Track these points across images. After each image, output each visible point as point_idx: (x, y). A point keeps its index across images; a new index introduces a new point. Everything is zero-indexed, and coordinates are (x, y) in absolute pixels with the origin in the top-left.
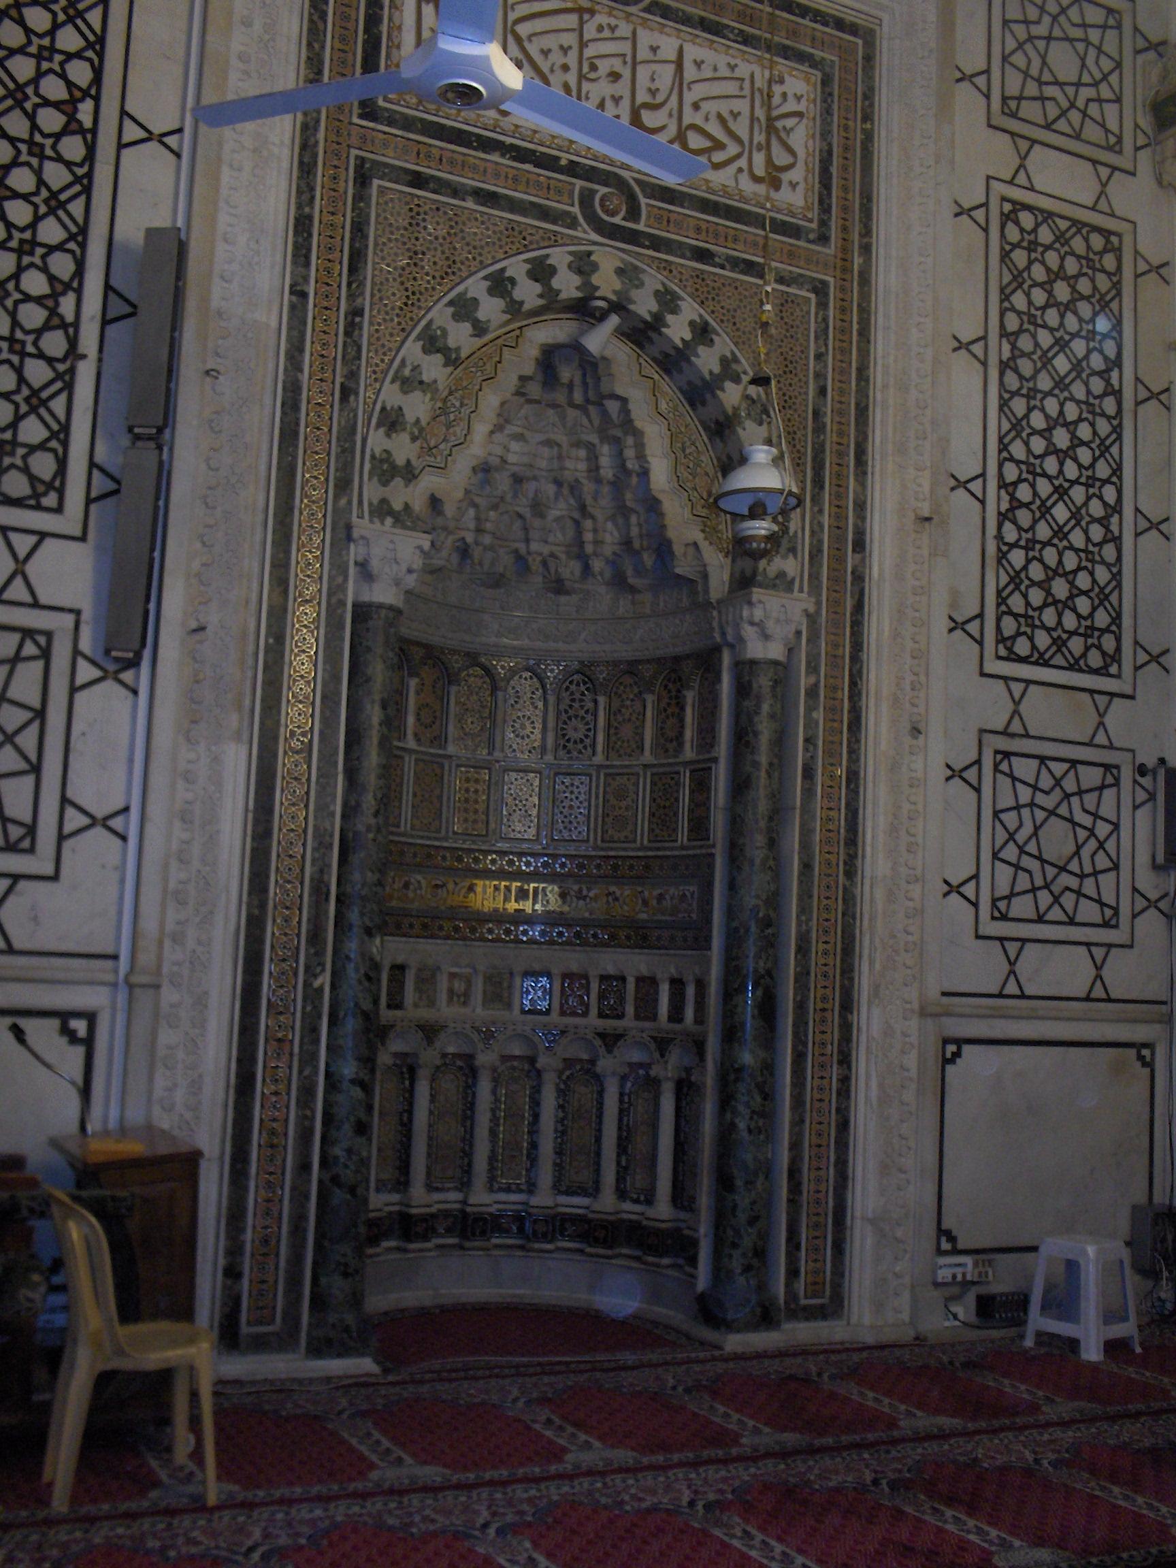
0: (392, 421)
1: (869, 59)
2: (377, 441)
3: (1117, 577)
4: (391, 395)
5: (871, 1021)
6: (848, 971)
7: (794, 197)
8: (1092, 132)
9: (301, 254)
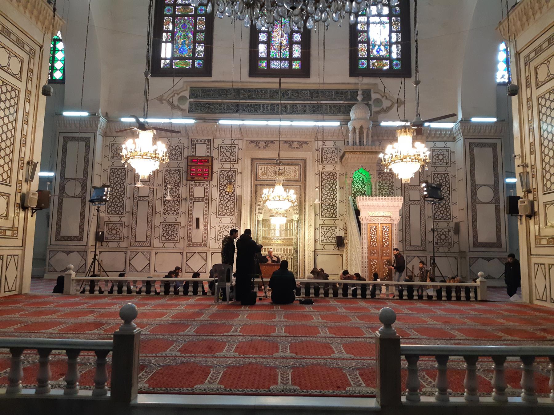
0: (259, 205)
1: (305, 162)
2: (258, 207)
3: (337, 208)
4: (259, 203)
5: (307, 252)
6: (304, 248)
7: (297, 177)
8: (333, 162)
9: (251, 193)
